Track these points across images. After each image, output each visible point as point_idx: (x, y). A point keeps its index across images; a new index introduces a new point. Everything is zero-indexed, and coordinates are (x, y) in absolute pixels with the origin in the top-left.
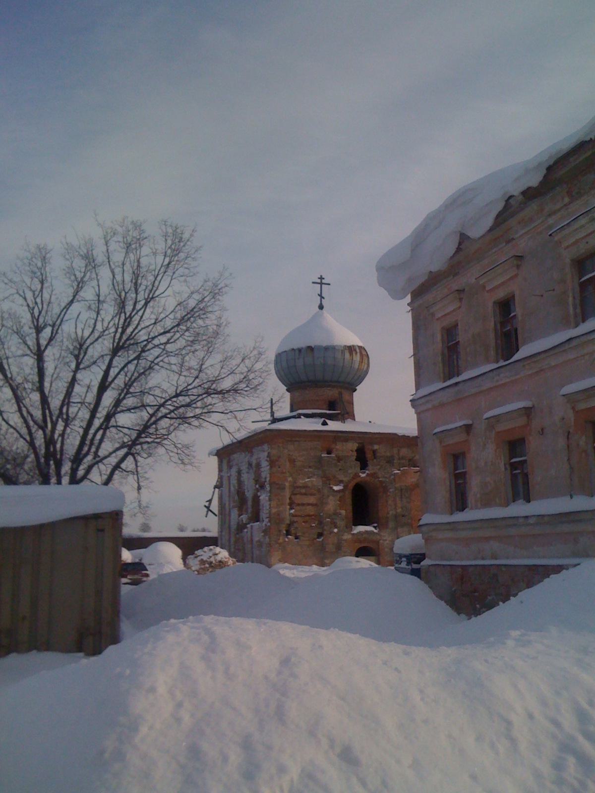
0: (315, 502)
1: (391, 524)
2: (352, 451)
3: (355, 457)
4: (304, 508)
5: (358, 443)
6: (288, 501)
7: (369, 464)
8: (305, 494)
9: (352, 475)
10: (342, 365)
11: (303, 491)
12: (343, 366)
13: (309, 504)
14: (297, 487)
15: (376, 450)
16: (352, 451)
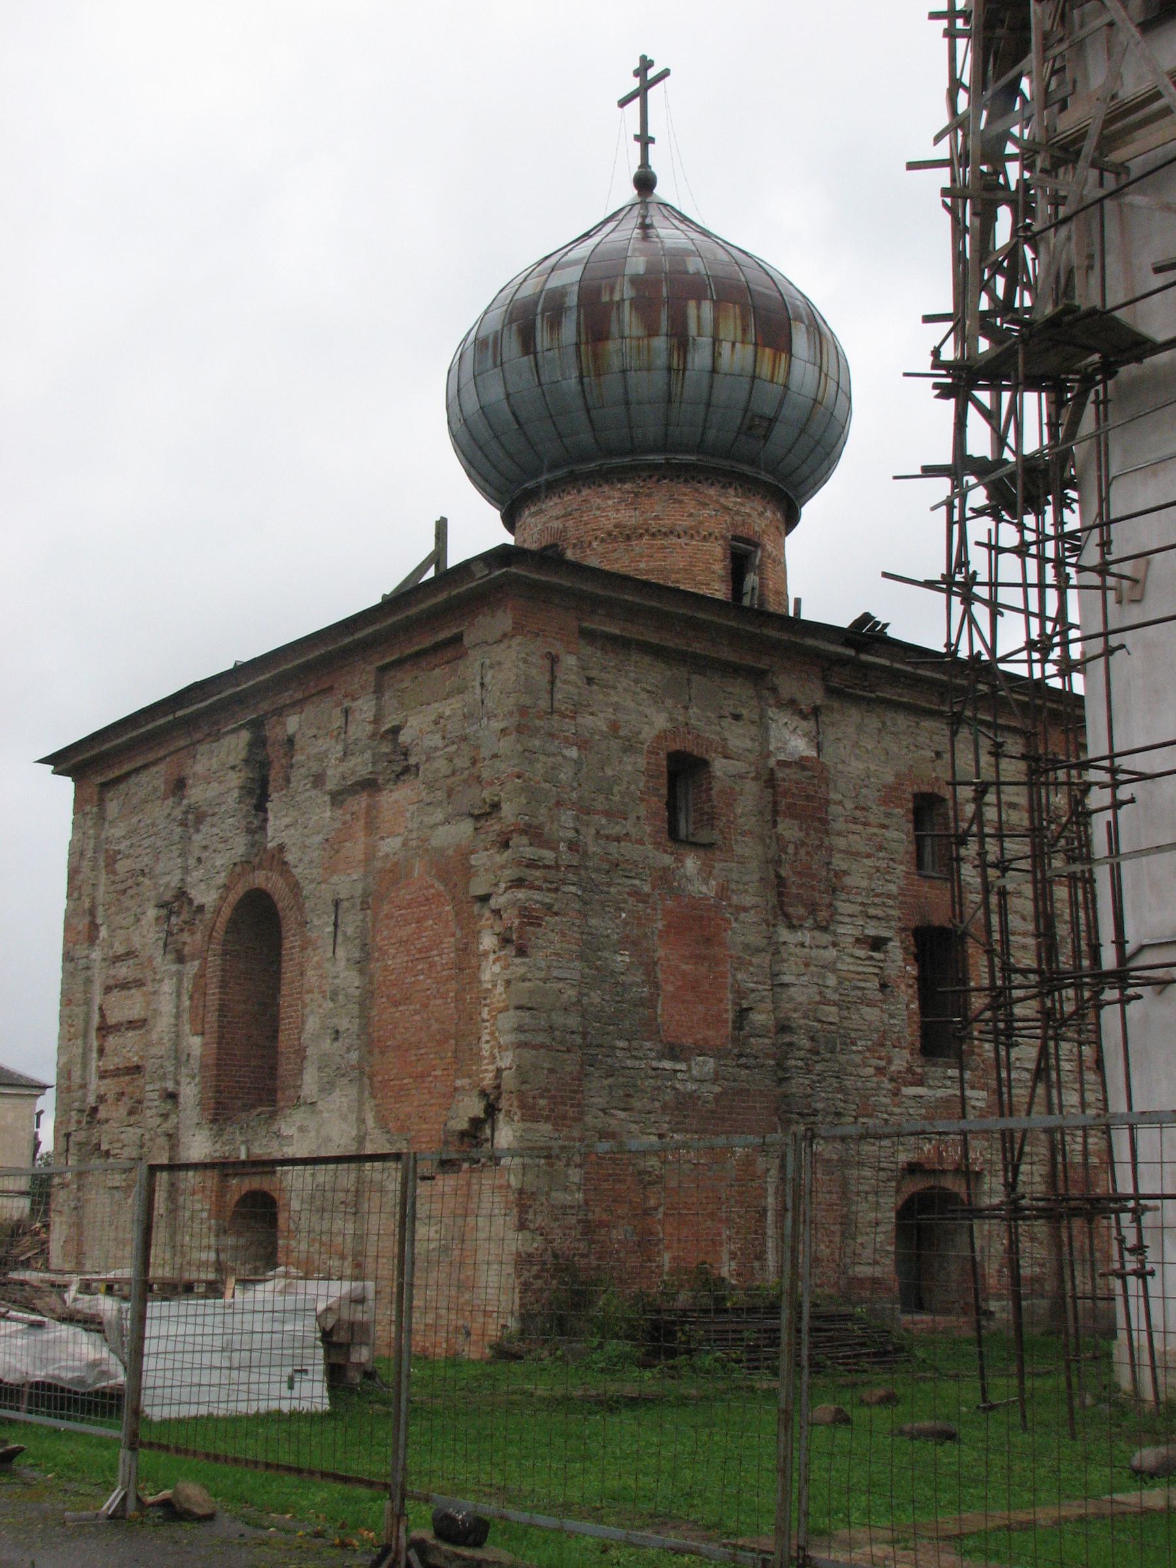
0: (143, 1015)
1: (310, 1081)
2: (233, 768)
3: (236, 794)
4: (121, 1040)
5: (256, 725)
6: (96, 1019)
7: (270, 815)
8: (124, 986)
9: (221, 879)
10: (502, 396)
11: (123, 971)
12: (508, 396)
13: (133, 1025)
14: (118, 959)
15: (294, 735)
16: (233, 768)
